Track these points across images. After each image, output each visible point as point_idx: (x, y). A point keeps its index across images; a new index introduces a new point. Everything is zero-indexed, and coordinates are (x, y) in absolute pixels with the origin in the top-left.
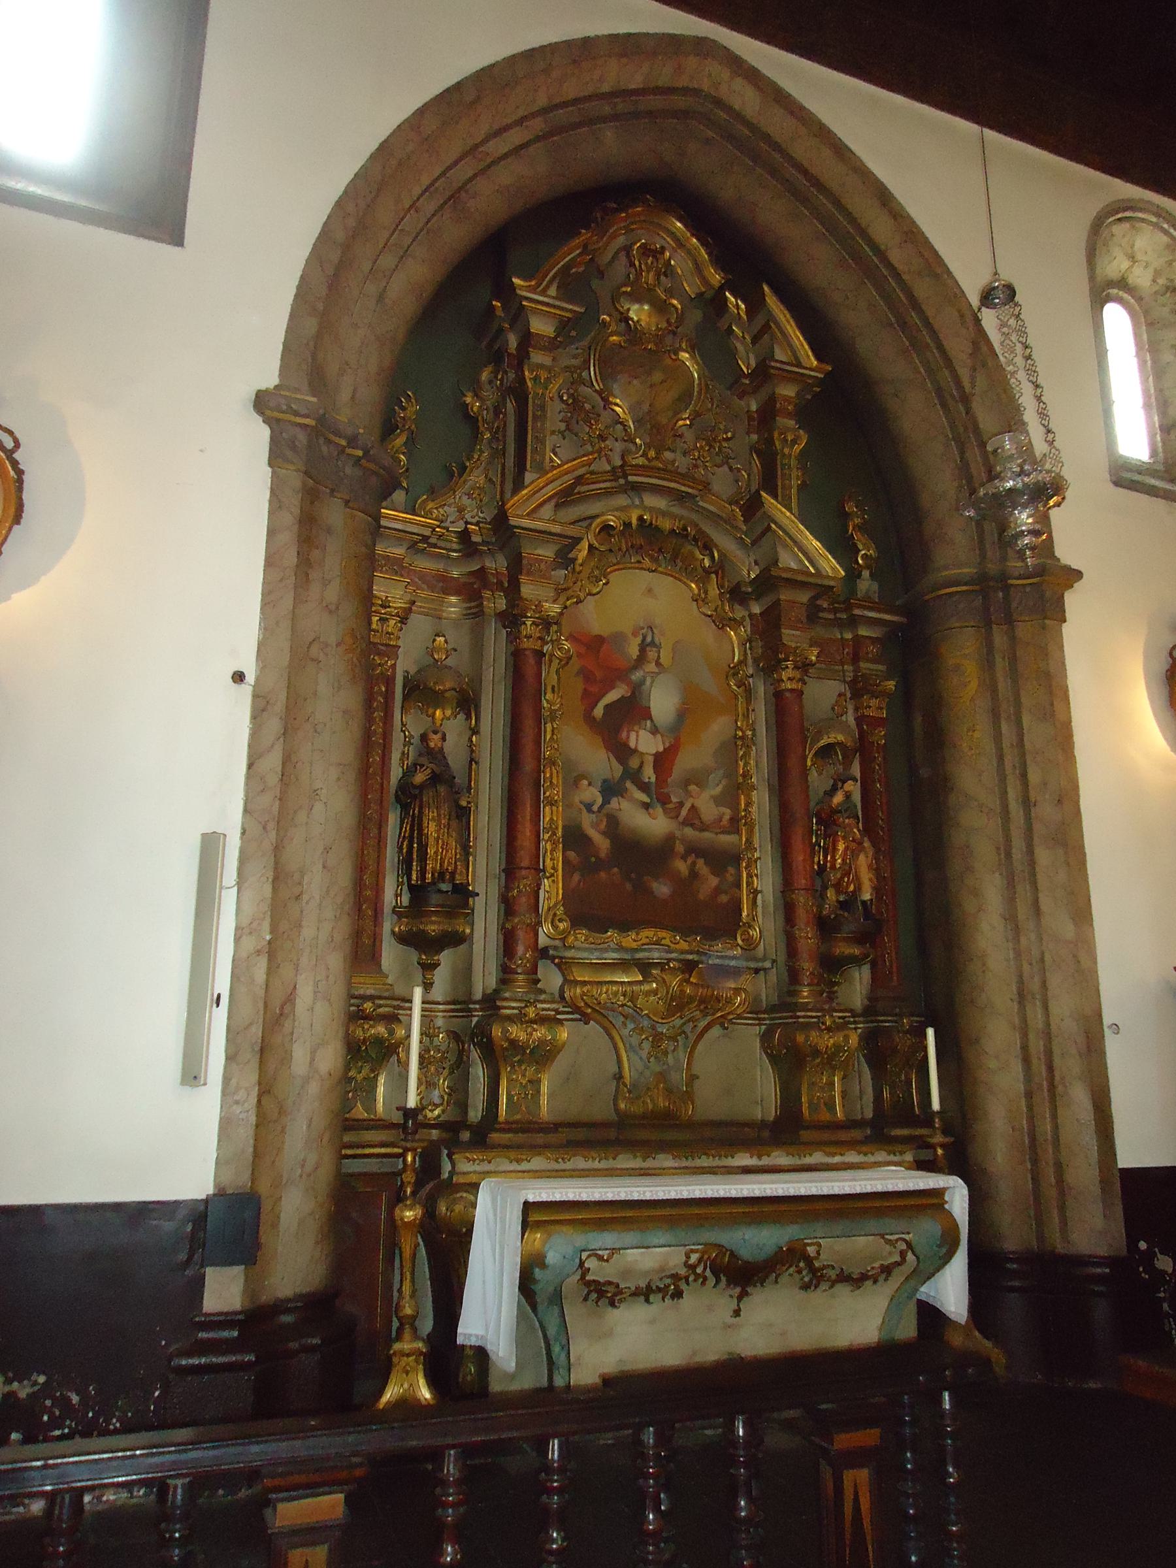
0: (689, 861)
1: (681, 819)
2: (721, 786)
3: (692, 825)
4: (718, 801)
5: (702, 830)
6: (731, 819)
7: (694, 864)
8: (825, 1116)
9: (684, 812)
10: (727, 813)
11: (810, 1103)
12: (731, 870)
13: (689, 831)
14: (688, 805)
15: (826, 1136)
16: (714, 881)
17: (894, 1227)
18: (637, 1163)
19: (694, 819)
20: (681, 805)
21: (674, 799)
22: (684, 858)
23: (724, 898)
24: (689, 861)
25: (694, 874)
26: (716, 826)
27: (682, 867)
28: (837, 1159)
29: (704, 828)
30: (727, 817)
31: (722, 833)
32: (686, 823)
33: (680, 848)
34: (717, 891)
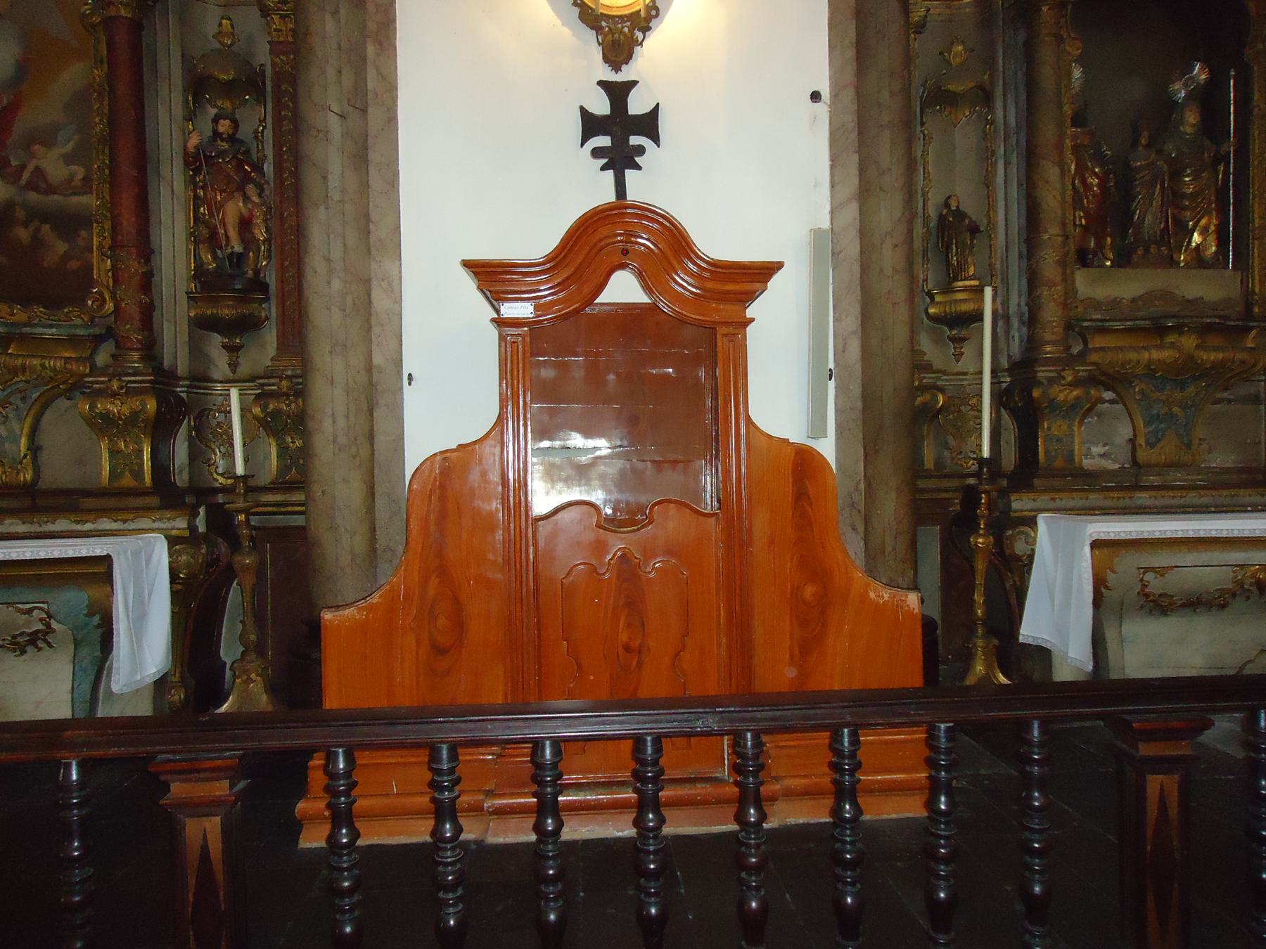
0: (31, 228)
1: (23, 182)
2: (71, 144)
3: (37, 189)
4: (69, 159)
5: (46, 193)
6: (84, 179)
7: (38, 229)
8: (127, 481)
9: (26, 175)
10: (80, 172)
11: (1047, 452)
12: (83, 233)
13: (33, 196)
14: (30, 168)
15: (112, 503)
16: (61, 247)
17: (27, 596)
18: (22, 528)
19: (39, 182)
20: (23, 167)
21: (14, 163)
22: (25, 224)
23: (74, 265)
24: (31, 228)
25: (37, 240)
26: (68, 187)
27: (23, 234)
28: (88, 526)
29: (50, 190)
30: (80, 176)
31: (75, 194)
32: (31, 186)
33: (20, 214)
34: (66, 257)
